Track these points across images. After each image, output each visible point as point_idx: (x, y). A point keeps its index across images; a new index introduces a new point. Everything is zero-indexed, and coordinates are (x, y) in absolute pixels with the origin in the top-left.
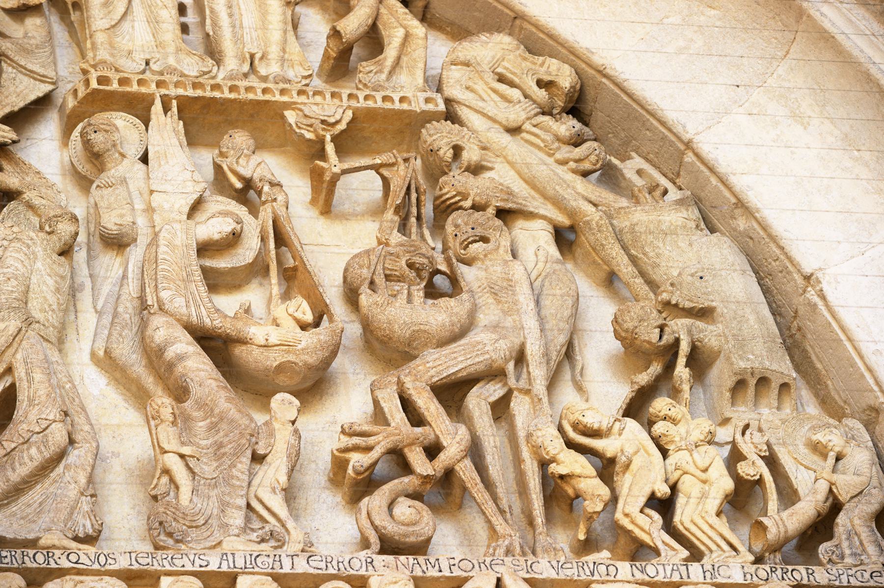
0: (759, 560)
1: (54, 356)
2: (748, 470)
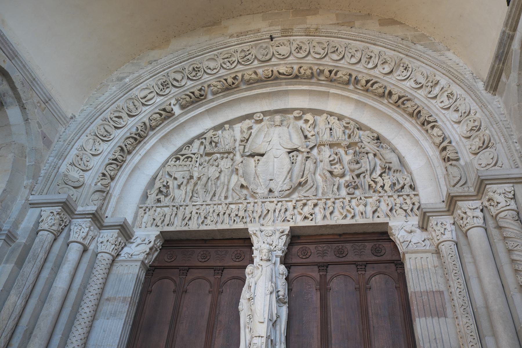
1: (313, 175)
2: (394, 182)
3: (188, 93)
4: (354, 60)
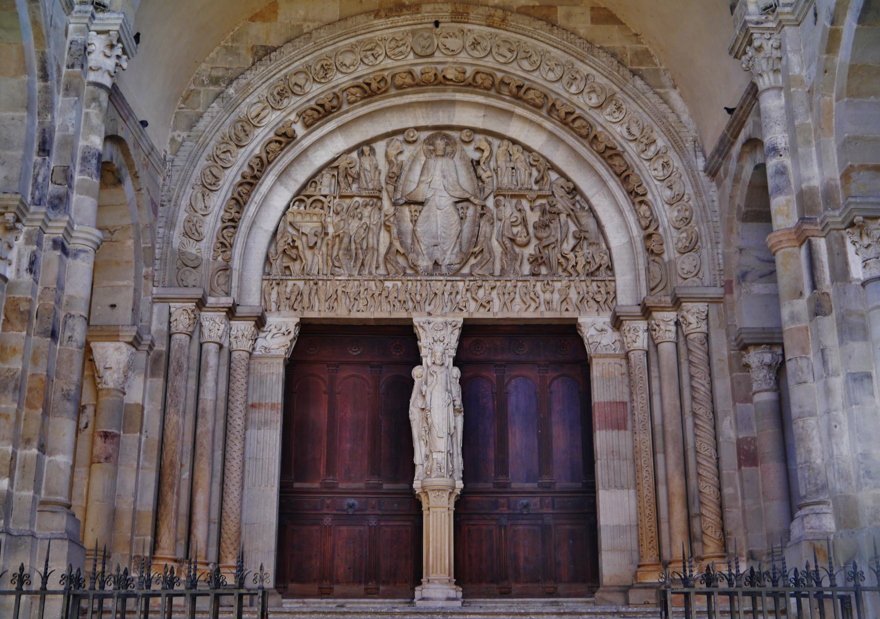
0: (587, 275)
2: (588, 260)
3: (312, 103)
4: (551, 76)
